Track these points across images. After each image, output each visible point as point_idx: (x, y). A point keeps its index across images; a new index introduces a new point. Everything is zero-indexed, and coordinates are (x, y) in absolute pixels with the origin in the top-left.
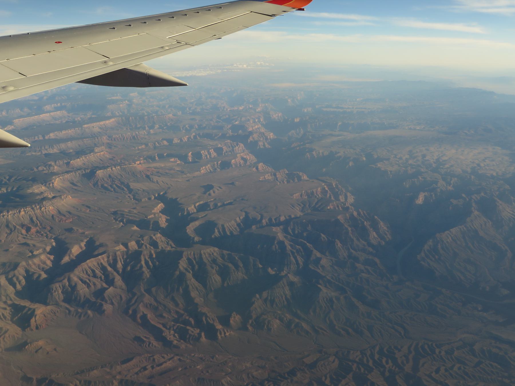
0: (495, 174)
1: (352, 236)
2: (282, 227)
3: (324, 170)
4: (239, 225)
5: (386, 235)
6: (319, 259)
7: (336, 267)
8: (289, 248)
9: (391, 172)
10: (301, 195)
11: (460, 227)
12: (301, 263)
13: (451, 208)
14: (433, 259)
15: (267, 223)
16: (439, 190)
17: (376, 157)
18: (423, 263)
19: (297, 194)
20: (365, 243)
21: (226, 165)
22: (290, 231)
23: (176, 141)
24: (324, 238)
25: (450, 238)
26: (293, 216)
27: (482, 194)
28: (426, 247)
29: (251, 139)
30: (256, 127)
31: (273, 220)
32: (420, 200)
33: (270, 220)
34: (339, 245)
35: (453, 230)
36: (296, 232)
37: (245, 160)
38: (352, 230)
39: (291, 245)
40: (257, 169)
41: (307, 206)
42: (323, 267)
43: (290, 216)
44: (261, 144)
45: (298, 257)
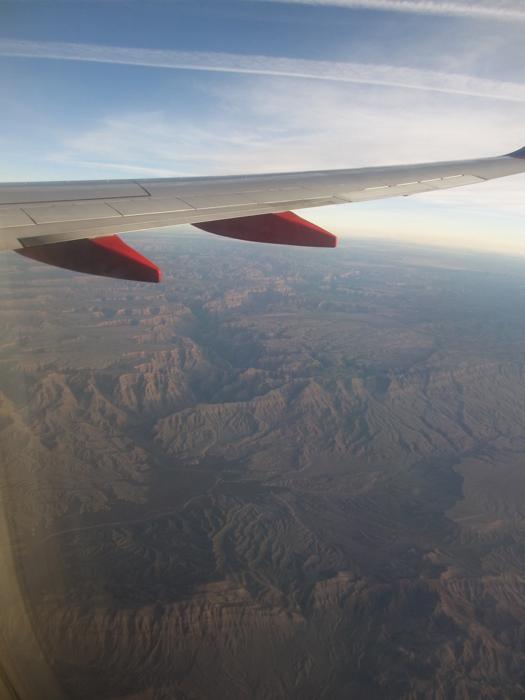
2: (68, 375)
4: (39, 368)
6: (62, 404)
8: (44, 390)
10: (138, 355)
11: (241, 403)
13: (260, 386)
14: (174, 425)
16: (279, 370)
17: (285, 334)
18: (156, 427)
19: (134, 353)
21: (135, 323)
22: (71, 381)
23: (137, 298)
25: (216, 411)
26: (92, 368)
28: (179, 414)
29: (207, 305)
30: (240, 296)
35: (228, 405)
37: (163, 322)
38: (128, 389)
39: (48, 390)
40: (152, 329)
41: (121, 363)
44: (211, 310)
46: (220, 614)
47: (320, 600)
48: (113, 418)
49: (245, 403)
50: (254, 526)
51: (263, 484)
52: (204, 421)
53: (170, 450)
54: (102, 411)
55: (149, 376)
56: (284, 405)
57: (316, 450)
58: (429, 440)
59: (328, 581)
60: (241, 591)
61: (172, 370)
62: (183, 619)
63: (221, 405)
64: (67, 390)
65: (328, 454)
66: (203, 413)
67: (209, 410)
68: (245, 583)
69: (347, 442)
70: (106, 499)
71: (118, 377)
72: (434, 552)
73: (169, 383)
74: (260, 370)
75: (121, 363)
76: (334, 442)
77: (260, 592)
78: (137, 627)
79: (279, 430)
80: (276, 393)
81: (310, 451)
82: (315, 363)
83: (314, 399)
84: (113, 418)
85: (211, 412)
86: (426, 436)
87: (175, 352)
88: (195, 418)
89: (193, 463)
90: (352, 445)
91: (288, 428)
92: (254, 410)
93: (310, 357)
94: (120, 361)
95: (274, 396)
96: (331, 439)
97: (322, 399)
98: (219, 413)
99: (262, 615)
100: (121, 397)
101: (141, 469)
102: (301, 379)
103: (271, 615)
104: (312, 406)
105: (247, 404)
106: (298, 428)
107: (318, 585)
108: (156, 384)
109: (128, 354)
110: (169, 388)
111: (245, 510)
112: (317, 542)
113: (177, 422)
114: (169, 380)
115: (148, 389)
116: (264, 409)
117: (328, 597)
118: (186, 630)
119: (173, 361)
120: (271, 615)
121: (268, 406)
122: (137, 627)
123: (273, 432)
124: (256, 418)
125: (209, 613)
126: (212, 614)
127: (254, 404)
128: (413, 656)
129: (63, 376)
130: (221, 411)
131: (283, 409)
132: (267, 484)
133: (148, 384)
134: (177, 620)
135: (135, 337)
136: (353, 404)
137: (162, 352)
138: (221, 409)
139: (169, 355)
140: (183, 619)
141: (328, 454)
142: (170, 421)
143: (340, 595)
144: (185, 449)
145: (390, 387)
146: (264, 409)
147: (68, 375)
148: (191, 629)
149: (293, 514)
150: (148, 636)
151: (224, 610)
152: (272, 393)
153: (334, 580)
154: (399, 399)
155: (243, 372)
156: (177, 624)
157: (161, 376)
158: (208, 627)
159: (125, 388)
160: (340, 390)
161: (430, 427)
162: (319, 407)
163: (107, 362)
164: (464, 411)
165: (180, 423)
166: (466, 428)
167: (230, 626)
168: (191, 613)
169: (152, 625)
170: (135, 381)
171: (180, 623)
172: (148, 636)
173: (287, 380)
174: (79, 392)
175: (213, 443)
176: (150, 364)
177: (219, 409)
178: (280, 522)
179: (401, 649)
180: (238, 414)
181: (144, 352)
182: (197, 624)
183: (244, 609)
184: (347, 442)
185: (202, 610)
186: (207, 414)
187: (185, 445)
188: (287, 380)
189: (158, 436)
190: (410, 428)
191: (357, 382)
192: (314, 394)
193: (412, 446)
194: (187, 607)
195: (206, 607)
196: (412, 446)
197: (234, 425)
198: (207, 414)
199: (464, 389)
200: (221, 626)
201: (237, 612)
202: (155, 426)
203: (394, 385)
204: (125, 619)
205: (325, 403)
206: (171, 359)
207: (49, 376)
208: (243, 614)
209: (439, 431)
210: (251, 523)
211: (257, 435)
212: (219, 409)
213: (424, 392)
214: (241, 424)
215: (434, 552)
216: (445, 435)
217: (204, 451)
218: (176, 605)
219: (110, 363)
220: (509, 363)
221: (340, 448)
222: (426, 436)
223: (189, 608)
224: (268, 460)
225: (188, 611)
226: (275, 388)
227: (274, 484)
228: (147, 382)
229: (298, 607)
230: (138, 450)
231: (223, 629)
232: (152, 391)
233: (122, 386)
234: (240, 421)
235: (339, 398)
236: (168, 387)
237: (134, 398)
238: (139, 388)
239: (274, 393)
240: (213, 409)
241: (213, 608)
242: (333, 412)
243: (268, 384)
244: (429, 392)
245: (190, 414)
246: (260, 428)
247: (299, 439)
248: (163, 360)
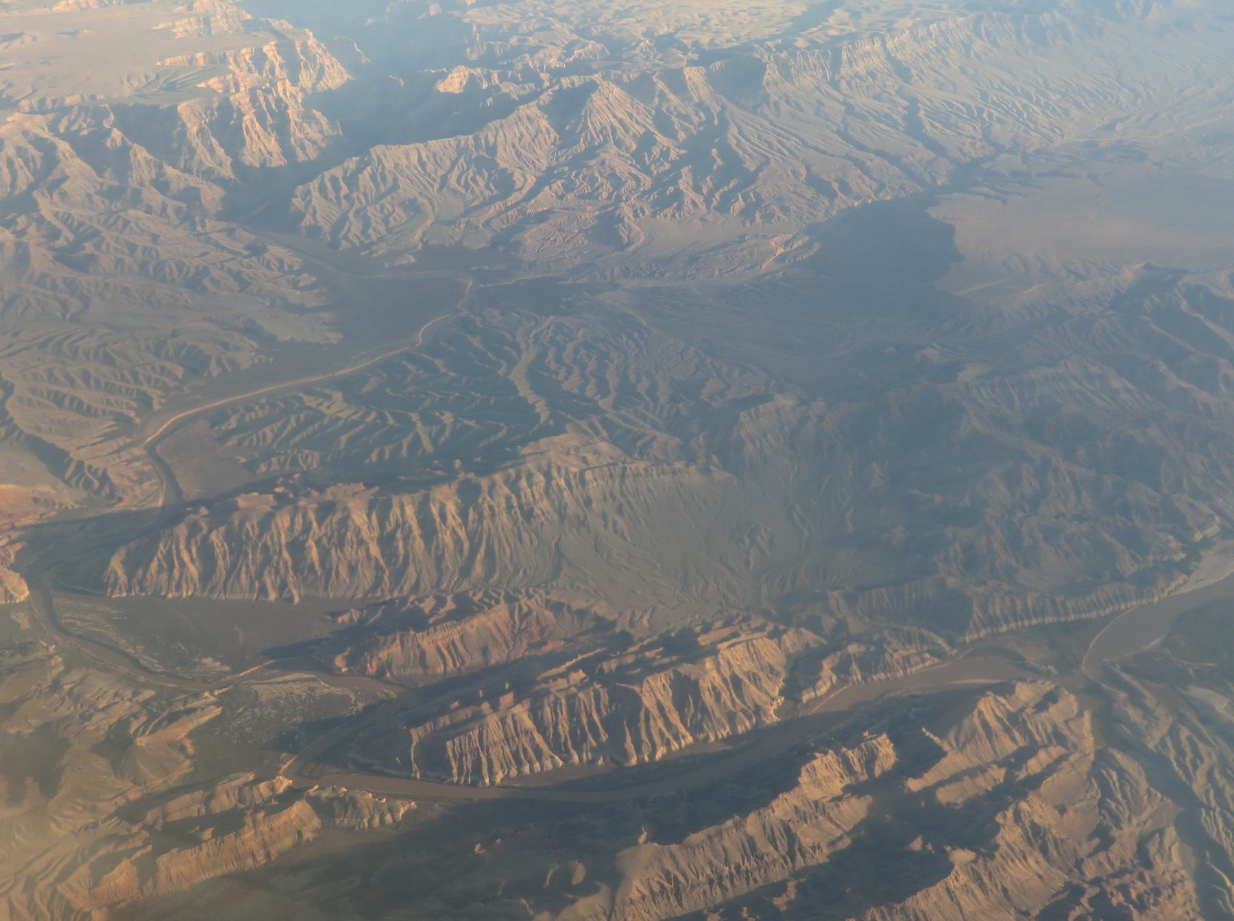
0: (705, 40)
1: (196, 142)
3: (370, 21)
5: (303, 147)
6: (64, 178)
7: (96, 198)
9: (479, 26)
11: (462, 137)
12: (22, 185)
13: (489, 101)
14: (332, 195)
15: (31, 107)
16: (520, 66)
18: (297, 202)
19: (179, 58)
20: (228, 161)
24: (113, 140)
25: (414, 158)
27: (597, 77)
28: (338, 172)
31: (49, 101)
32: (454, 83)
33: (42, 102)
34: (140, 154)
35: (435, 144)
36: (75, 127)
39: (20, 151)
41: (162, 80)
42: (64, 195)
43: (93, 97)
45: (20, 173)
46: (583, 482)
47: (753, 442)
48: (190, 196)
49: (470, 137)
50: (576, 351)
51: (563, 283)
52: (395, 180)
53: (344, 244)
54: (161, 185)
55: (240, 98)
56: (554, 134)
57: (647, 213)
58: (867, 172)
59: (761, 407)
60: (604, 446)
61: (280, 89)
62: (519, 497)
63: (421, 146)
64: (63, 146)
65: (673, 216)
66: (389, 165)
67: (396, 157)
68: (605, 434)
69: (705, 191)
70: (255, 345)
71: (176, 107)
72: (932, 347)
73: (289, 111)
74: (479, 70)
75: (162, 80)
76: (679, 194)
77: (639, 443)
78: (438, 519)
79: (559, 183)
80: (531, 109)
81: (636, 215)
82: (590, 47)
83: (615, 116)
84: (190, 196)
85: (405, 161)
86: (860, 165)
87: (269, 49)
88: (373, 177)
89: (404, 262)
90: (717, 195)
91: (577, 175)
92: (492, 150)
93: (575, 37)
94: (158, 77)
95: (528, 118)
96: (671, 189)
97: (631, 116)
98: (423, 164)
99: (658, 475)
100: (193, 152)
101: (301, 284)
102: (575, 78)
103: (674, 473)
104: (614, 130)
105: (476, 139)
106: (597, 175)
107: (744, 416)
108: (261, 118)
109: (168, 62)
110: (293, 124)
111: (548, 328)
112: (709, 360)
113: (337, 189)
114: (286, 107)
115: (247, 128)
116: (514, 146)
117: (765, 435)
118: (529, 515)
119: (272, 71)
120: (674, 473)
121: (520, 140)
122: (438, 519)
123: (547, 188)
124: (503, 165)
125: (562, 483)
126: (568, 483)
127: (491, 140)
128: (938, 499)
129: (39, 118)
130: (425, 158)
131: (553, 144)
132: (570, 281)
133: (246, 118)
134: (508, 499)
135: (161, 26)
136: (696, 119)
137: (244, 51)
138: (423, 154)
139: (259, 59)
140: (519, 497)
141: (673, 216)
142: (322, 189)
143: (786, 429)
144: (374, 237)
145: (766, 77)
146: (514, 146)
147: (50, 117)
148: (537, 511)
149: (644, 323)
150: (462, 533)
151: (589, 475)
152: (523, 110)
153: (769, 405)
154: (787, 102)
155: (443, 76)
156: (509, 507)
157: (266, 100)
158: (566, 505)
159: (195, 130)
160: (662, 95)
161: (861, 147)
162: (627, 130)
163: (128, 80)
164: (921, 114)
165: (345, 190)
166: (932, 144)
167: (605, 499)
168: (530, 486)
169: (463, 514)
170: (212, 115)
171: (515, 504)
172: (462, 533)
173: (547, 84)
174: (90, 149)
175: (429, 222)
176: (229, 77)
177: (419, 154)
178: (625, 338)
179: (915, 492)
180: (462, 160)
181: (200, 55)
182: (545, 504)
183: (624, 469)
184: (705, 191)
185: (548, 475)
186: (396, 166)
187: (370, 231)
188: (547, 84)
189: (308, 220)
190: (824, 152)
191: (693, 75)
192: (610, 106)
193: (835, 186)
194: (518, 477)
195: (555, 474)
196: (835, 186)
197: (458, 181)
198: (396, 166)
199: (914, 72)
200: (588, 502)
201: (611, 476)
202: (294, 200)
203: (771, 74)
204: (410, 511)
205: (637, 122)
206: (267, 67)
207: (9, 119)
208: (623, 477)
209: (879, 153)
210: (570, 347)
211: (514, 198)
212: (419, 154)
213: (834, 84)
214: (473, 179)
215: (932, 347)
216: (894, 160)
217: (418, 236)
218: (498, 477)
219: (136, 84)
220: (994, 14)
221: (694, 204)
222: (860, 165)
223: (524, 479)
224: (555, 241)
225: (523, 483)
226: (524, 100)
227: (585, 280)
228: (241, 115)
229: (715, 458)
230: (275, 251)
231: (594, 505)
232: (256, 133)
233: (189, 125)
234: (471, 174)
235: (664, 109)
236: (289, 121)
237: (220, 151)
238: (226, 126)
239: (528, 112)
240: (408, 157)
241: (567, 473)
242: (660, 138)
243: (508, 94)
244: (843, 85)
245: (359, 170)
246: (518, 184)
247: (605, 195)
248: (250, 70)
